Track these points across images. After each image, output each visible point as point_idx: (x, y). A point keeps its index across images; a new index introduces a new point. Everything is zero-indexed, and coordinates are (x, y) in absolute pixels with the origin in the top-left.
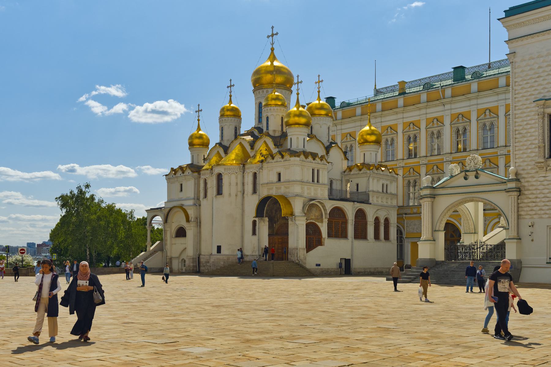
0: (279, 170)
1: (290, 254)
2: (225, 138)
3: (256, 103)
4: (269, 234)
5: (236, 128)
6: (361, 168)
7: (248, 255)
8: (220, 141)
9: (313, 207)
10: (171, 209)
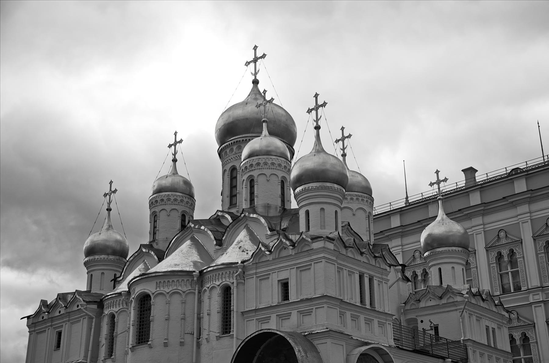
0: (283, 275)
2: (159, 236)
3: (224, 172)
5: (183, 216)
8: (150, 242)
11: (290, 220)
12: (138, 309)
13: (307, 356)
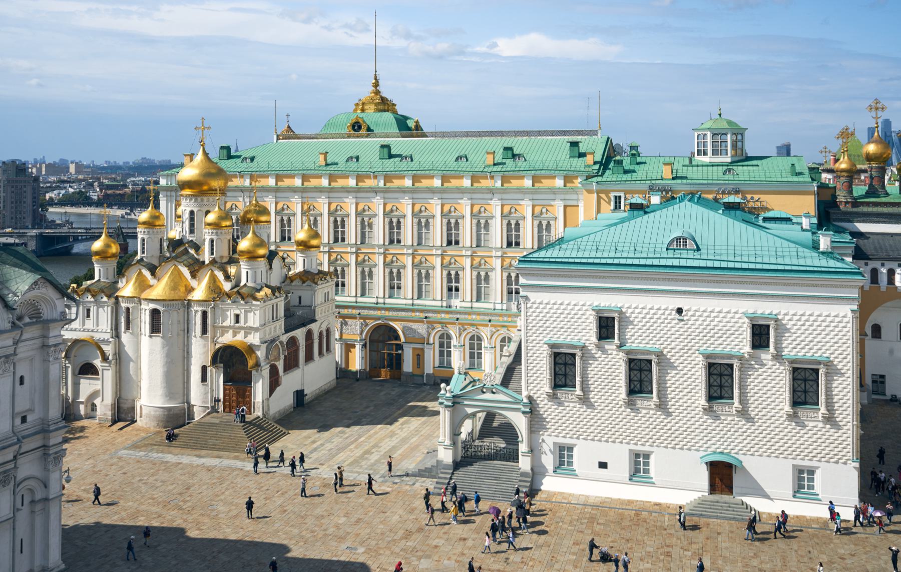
0: (237, 312)
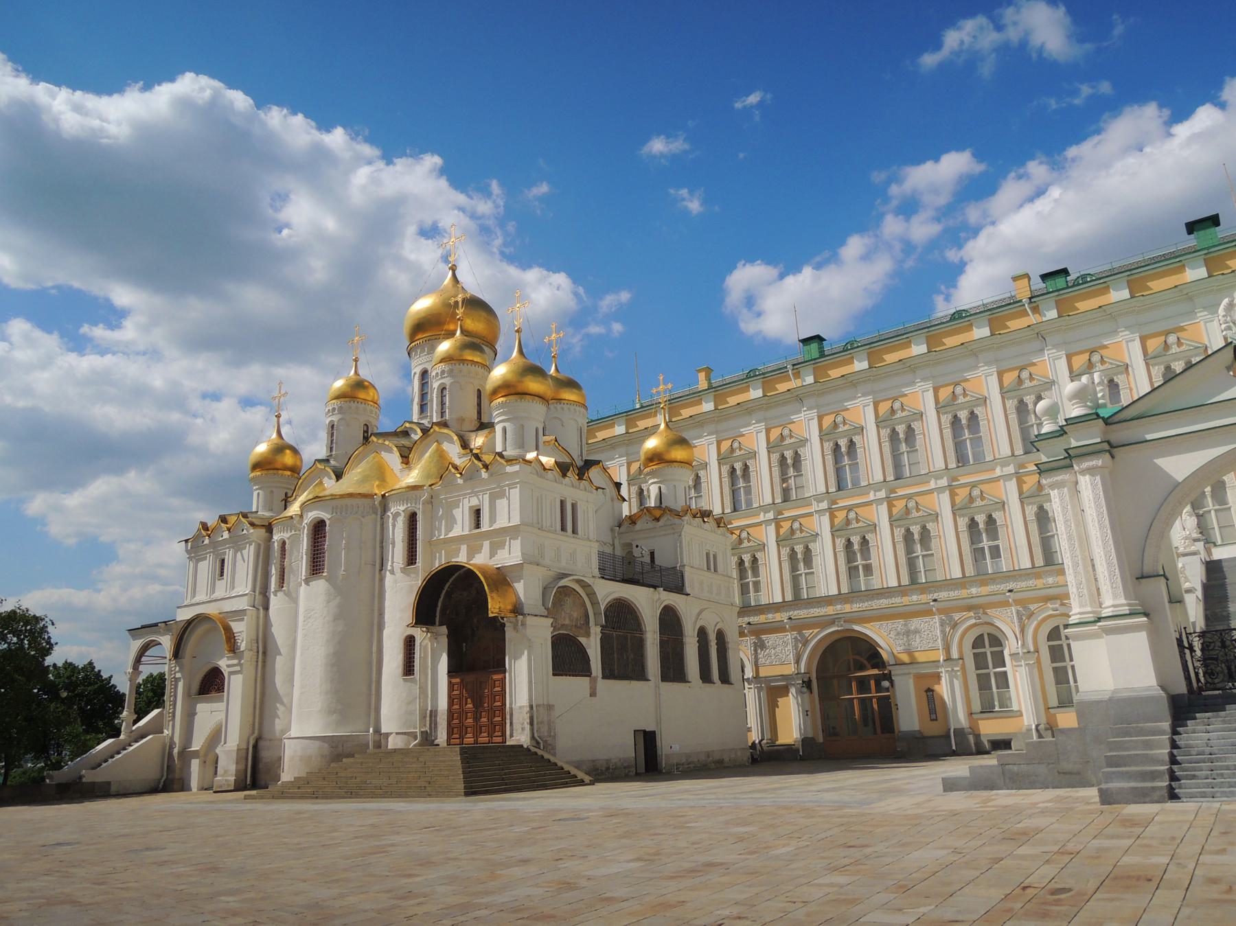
0: (474, 502)
1: (511, 724)
4: (449, 672)
6: (658, 516)
7: (392, 733)
9: (566, 595)
10: (189, 623)
11: (486, 437)
12: (311, 536)
13: (498, 591)
